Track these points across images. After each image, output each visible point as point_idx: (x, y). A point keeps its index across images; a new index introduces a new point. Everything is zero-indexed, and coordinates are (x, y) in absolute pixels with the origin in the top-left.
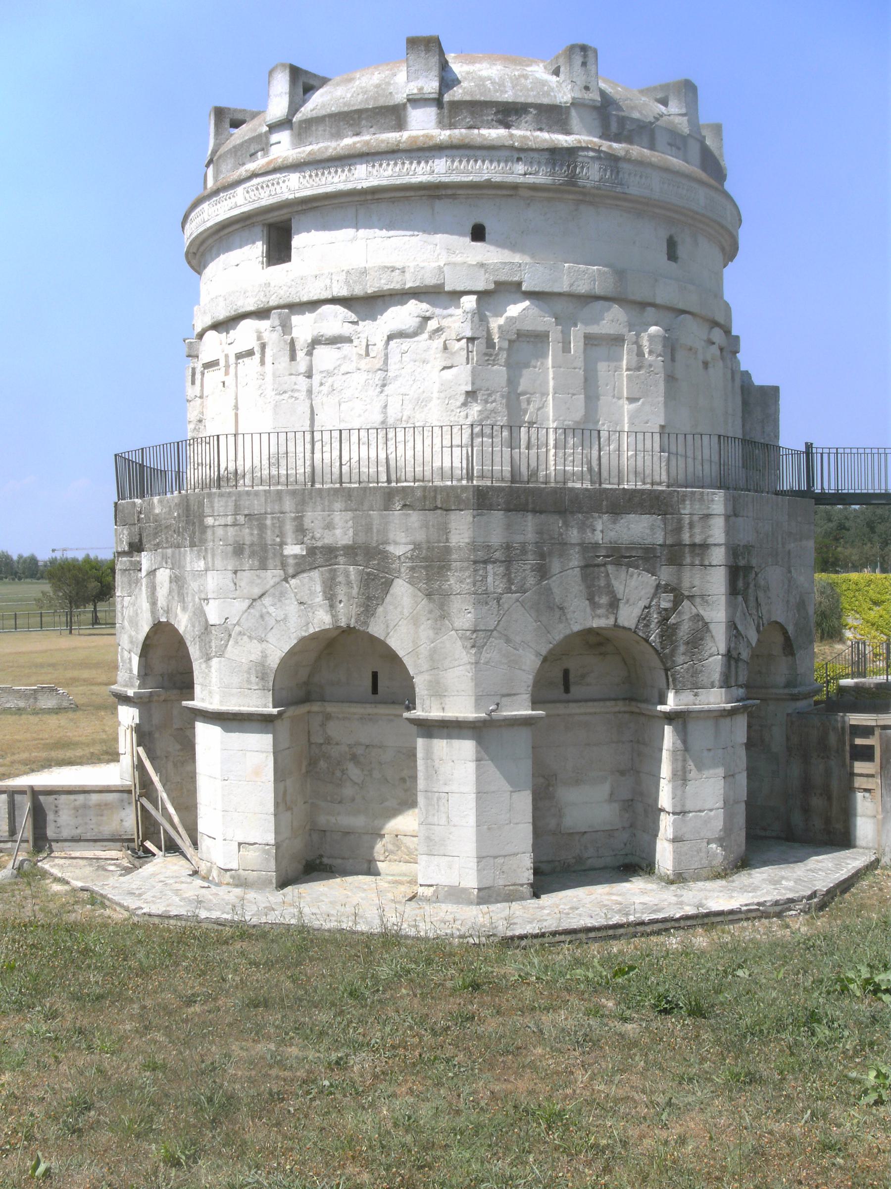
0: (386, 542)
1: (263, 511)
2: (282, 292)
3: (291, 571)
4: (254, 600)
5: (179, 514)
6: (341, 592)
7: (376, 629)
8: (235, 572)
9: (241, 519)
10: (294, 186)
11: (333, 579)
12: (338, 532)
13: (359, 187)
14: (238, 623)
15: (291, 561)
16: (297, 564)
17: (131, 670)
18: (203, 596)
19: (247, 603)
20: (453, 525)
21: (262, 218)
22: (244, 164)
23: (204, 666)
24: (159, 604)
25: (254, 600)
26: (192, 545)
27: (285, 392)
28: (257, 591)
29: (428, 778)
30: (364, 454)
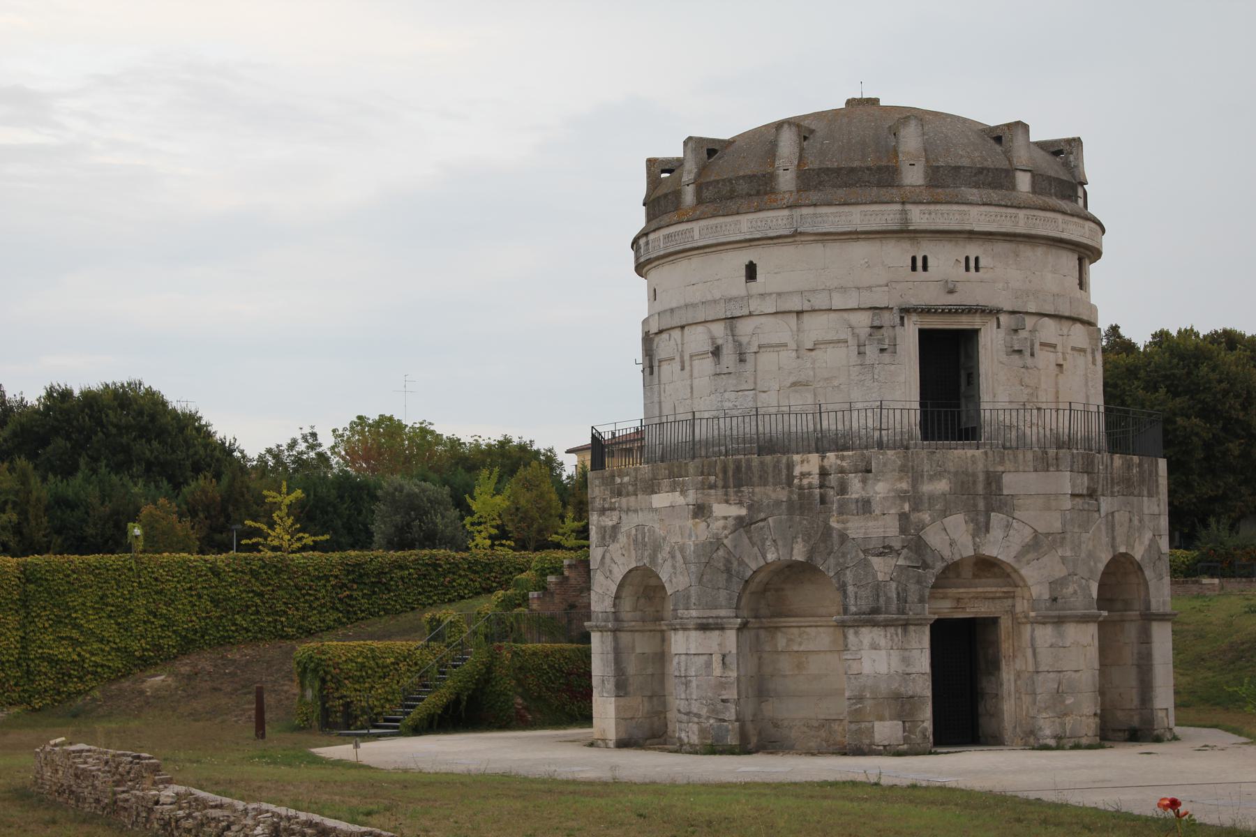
17: (1090, 595)
24: (1118, 540)
26: (1150, 495)
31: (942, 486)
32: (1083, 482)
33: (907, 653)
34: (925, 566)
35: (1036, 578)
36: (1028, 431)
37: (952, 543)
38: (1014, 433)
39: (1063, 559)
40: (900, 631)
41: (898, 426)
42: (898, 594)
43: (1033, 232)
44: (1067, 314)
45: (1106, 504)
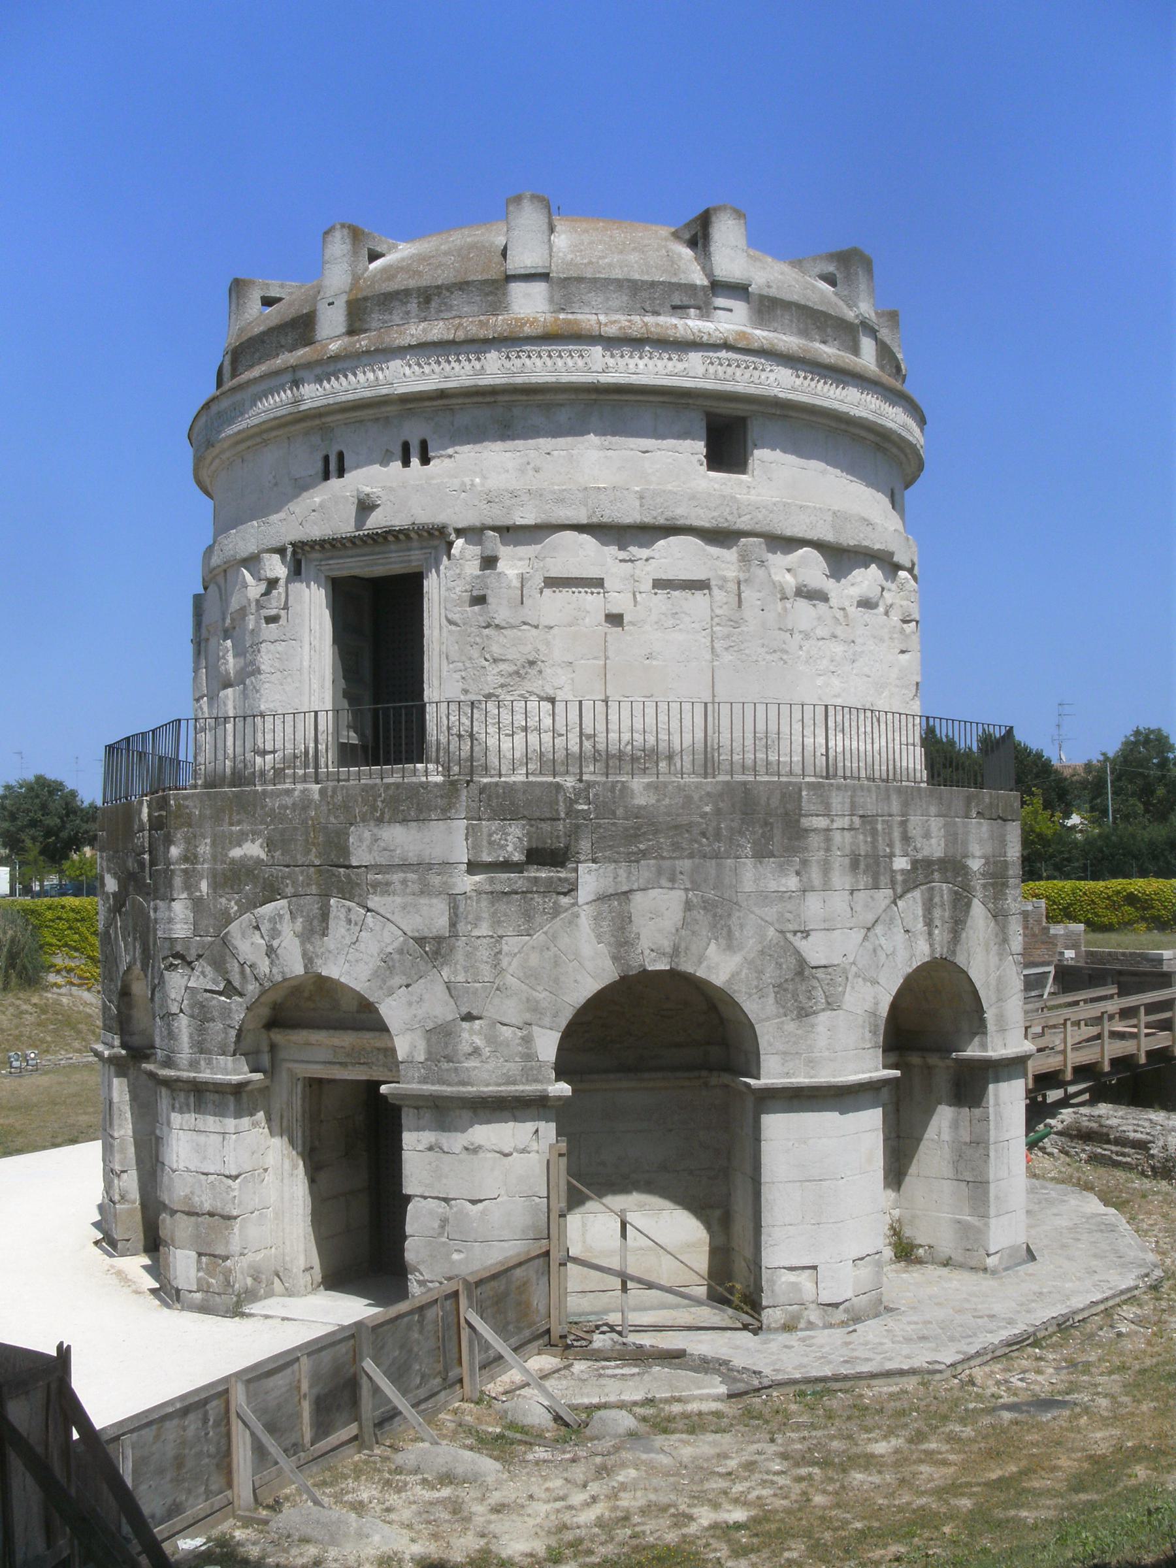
0: (966, 856)
1: (875, 812)
2: (760, 516)
3: (899, 891)
4: (869, 929)
5: (718, 812)
6: (937, 913)
7: (960, 960)
8: (852, 892)
9: (857, 820)
10: (780, 382)
11: (931, 899)
12: (933, 841)
13: (852, 413)
14: (854, 963)
15: (899, 878)
16: (905, 882)
17: (529, 1056)
18: (791, 927)
19: (863, 931)
20: (1008, 838)
21: (708, 403)
22: (656, 313)
23: (791, 1026)
24: (644, 944)
25: (869, 929)
26: (761, 854)
27: (775, 651)
28: (871, 918)
29: (996, 1128)
30: (862, 748)
31: (253, 849)
32: (512, 841)
33: (202, 1138)
34: (230, 990)
35: (408, 1018)
36: (506, 744)
37: (271, 952)
38: (466, 746)
39: (449, 986)
40: (192, 1099)
41: (289, 746)
42: (191, 1036)
43: (519, 380)
44: (628, 520)
45: (591, 879)
